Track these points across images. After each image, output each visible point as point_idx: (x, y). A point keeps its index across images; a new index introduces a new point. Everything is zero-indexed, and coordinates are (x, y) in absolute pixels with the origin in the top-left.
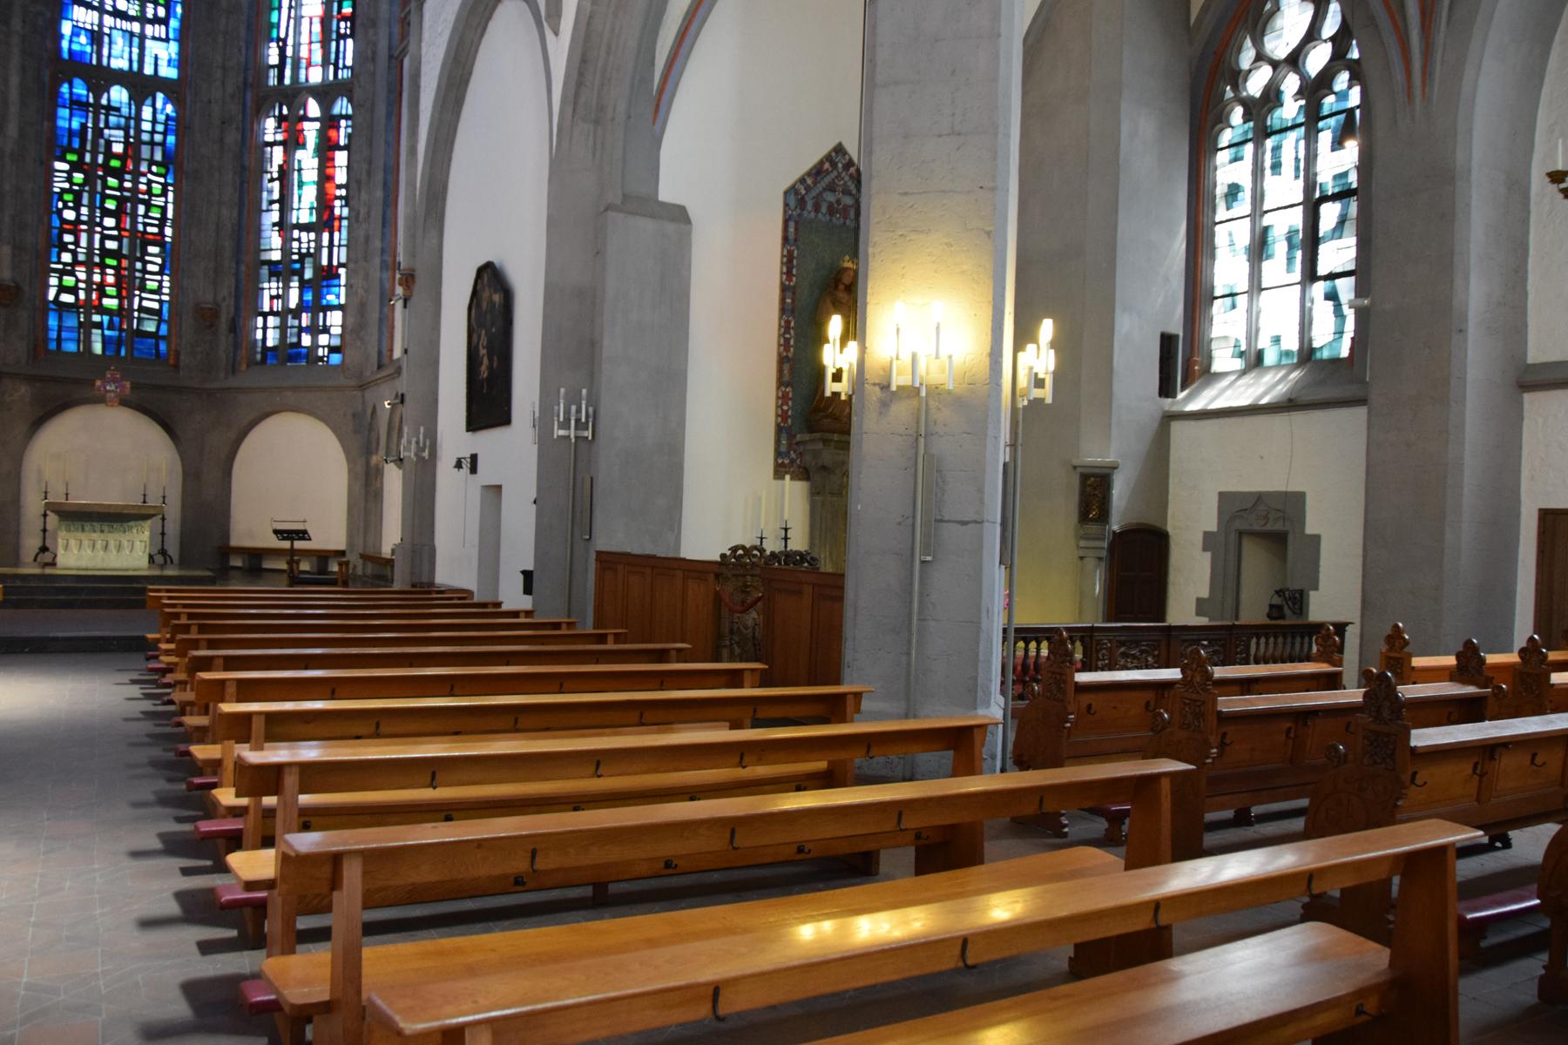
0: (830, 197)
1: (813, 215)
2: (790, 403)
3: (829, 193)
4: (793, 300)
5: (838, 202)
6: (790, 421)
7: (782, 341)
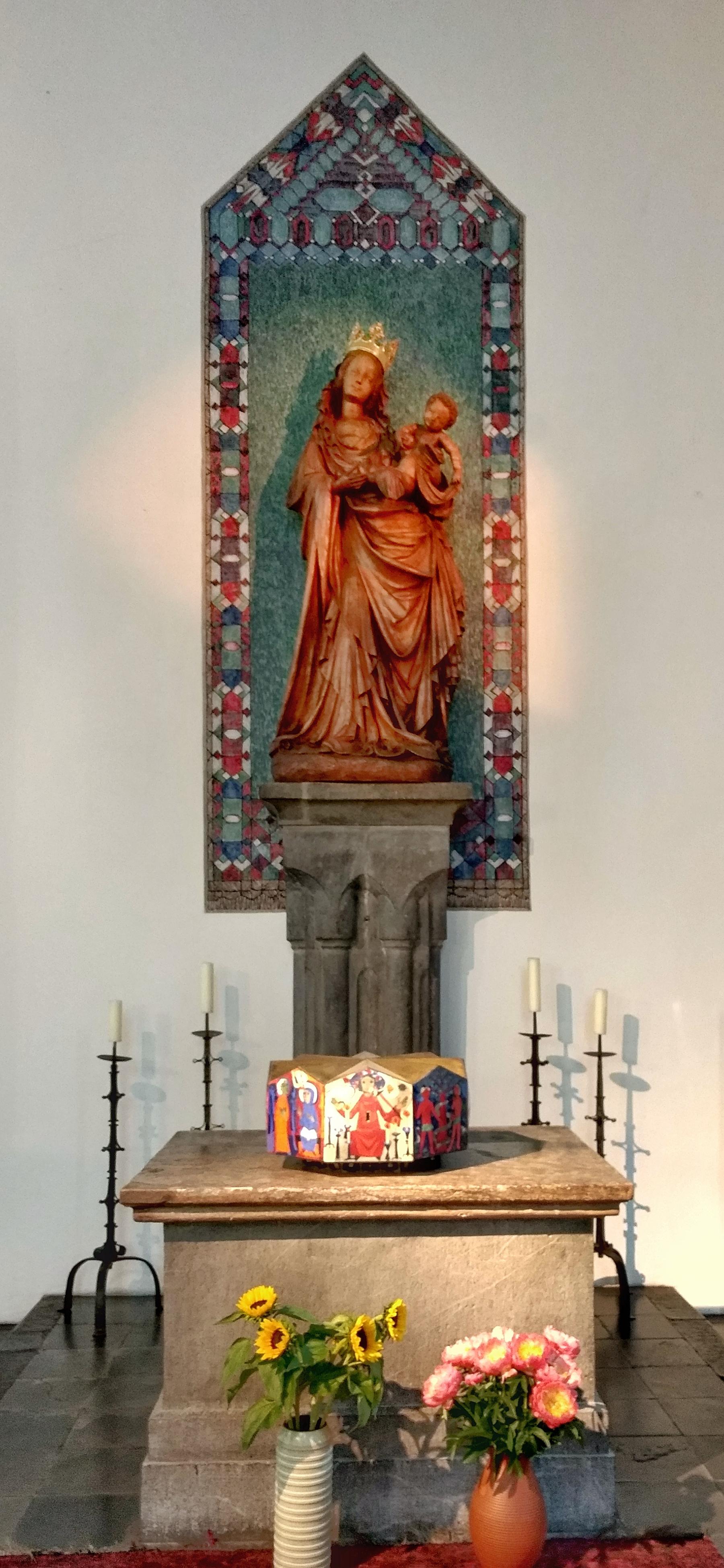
1: (290, 252)
2: (246, 722)
3: (335, 191)
4: (244, 470)
6: (246, 766)
7: (216, 573)
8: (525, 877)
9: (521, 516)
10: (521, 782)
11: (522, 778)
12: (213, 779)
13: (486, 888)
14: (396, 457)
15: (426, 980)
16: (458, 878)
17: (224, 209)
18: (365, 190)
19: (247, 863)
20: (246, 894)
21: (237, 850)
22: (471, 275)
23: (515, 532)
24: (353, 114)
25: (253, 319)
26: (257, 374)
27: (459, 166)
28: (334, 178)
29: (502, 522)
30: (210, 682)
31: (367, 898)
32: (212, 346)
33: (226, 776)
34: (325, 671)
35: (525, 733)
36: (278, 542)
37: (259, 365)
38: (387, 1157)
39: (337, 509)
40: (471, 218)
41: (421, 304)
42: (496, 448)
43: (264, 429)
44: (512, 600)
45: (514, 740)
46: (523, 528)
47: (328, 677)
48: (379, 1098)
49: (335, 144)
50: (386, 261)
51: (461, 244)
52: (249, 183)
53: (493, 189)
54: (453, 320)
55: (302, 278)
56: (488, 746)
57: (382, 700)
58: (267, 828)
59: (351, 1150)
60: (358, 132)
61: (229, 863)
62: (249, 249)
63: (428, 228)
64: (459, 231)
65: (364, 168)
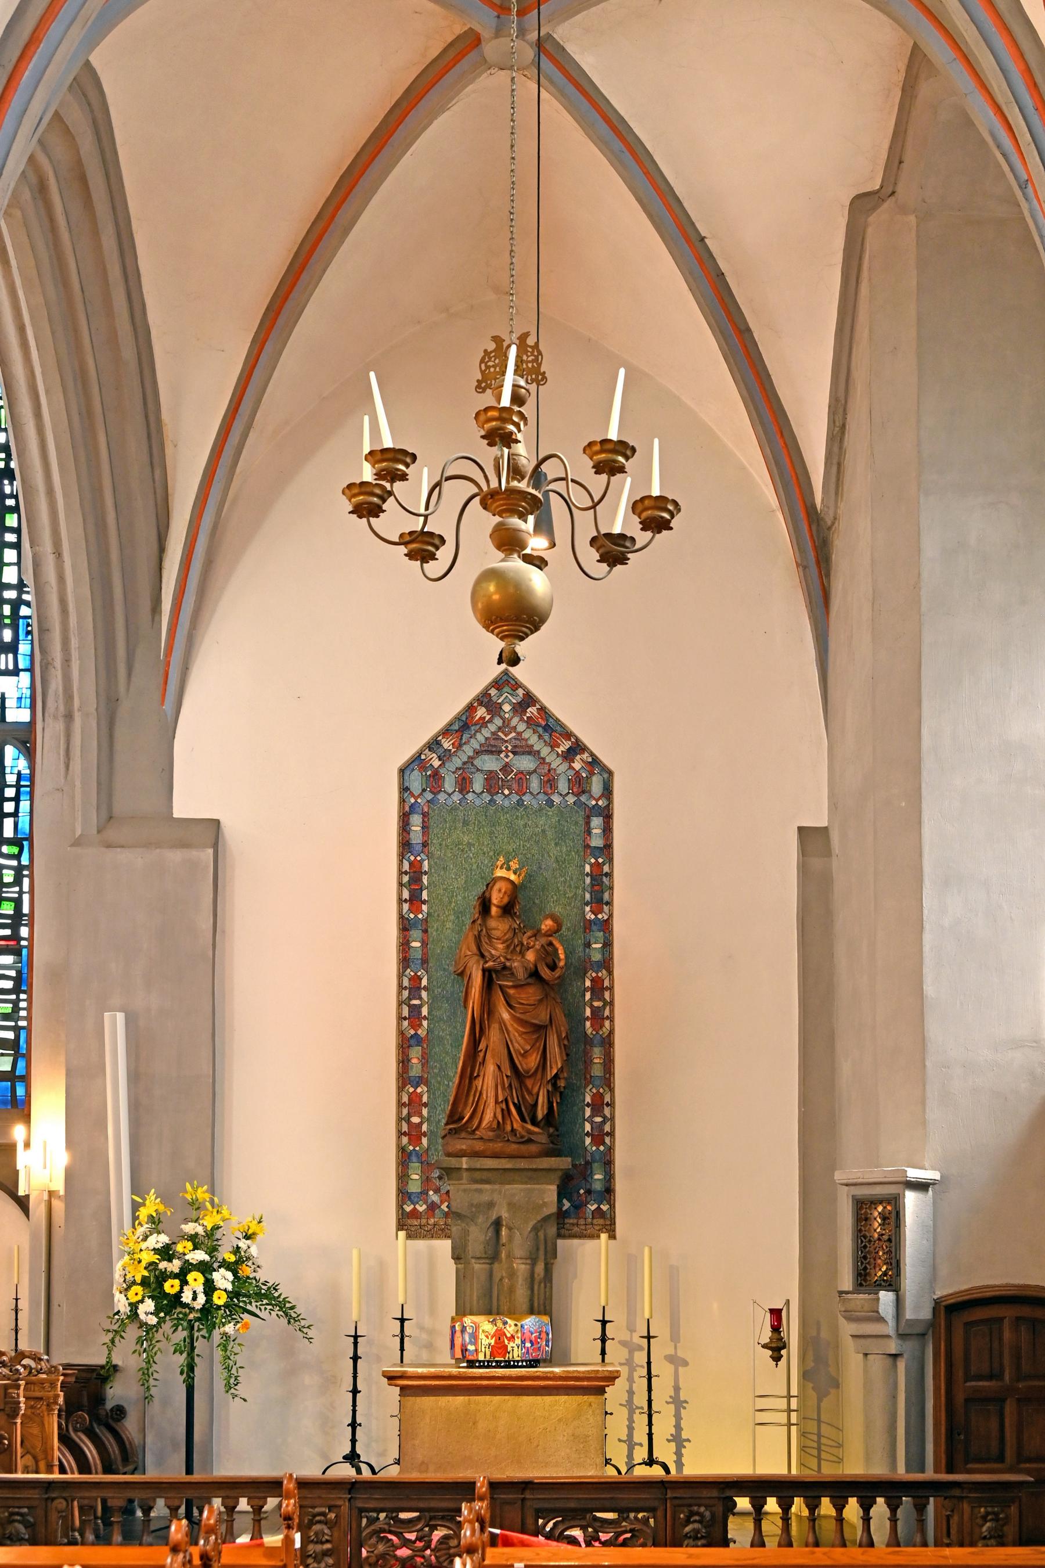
0: (490, 763)
1: (457, 797)
3: (486, 757)
4: (424, 944)
5: (506, 768)
6: (425, 1141)
7: (406, 1012)
8: (613, 1216)
9: (610, 973)
10: (610, 1152)
11: (611, 1149)
12: (402, 1150)
13: (586, 1224)
14: (522, 954)
15: (542, 1285)
16: (566, 1218)
17: (413, 770)
18: (507, 756)
19: (424, 1207)
20: (423, 1227)
21: (418, 1197)
22: (577, 812)
23: (606, 983)
24: (500, 706)
25: (432, 842)
26: (434, 879)
27: (570, 740)
28: (486, 748)
29: (597, 976)
30: (400, 1085)
31: (504, 1232)
32: (404, 861)
33: (411, 1148)
34: (478, 1083)
35: (612, 1119)
36: (447, 991)
37: (435, 873)
38: (509, 1358)
39: (486, 980)
40: (577, 772)
41: (543, 831)
42: (594, 928)
43: (438, 916)
44: (604, 1029)
45: (605, 1124)
46: (612, 981)
47: (479, 1088)
48: (505, 1330)
49: (487, 727)
50: (521, 803)
51: (571, 791)
52: (430, 753)
53: (592, 754)
54: (565, 842)
55: (464, 815)
56: (588, 1127)
57: (514, 1104)
58: (438, 1183)
59: (491, 1354)
60: (502, 718)
61: (412, 1206)
62: (429, 796)
63: (549, 781)
64: (569, 782)
65: (506, 741)
